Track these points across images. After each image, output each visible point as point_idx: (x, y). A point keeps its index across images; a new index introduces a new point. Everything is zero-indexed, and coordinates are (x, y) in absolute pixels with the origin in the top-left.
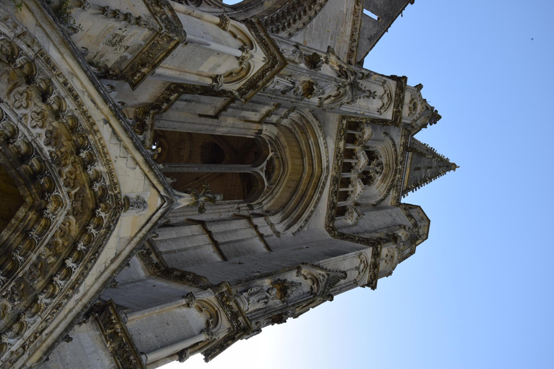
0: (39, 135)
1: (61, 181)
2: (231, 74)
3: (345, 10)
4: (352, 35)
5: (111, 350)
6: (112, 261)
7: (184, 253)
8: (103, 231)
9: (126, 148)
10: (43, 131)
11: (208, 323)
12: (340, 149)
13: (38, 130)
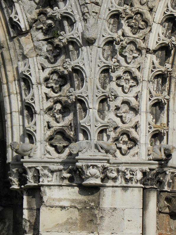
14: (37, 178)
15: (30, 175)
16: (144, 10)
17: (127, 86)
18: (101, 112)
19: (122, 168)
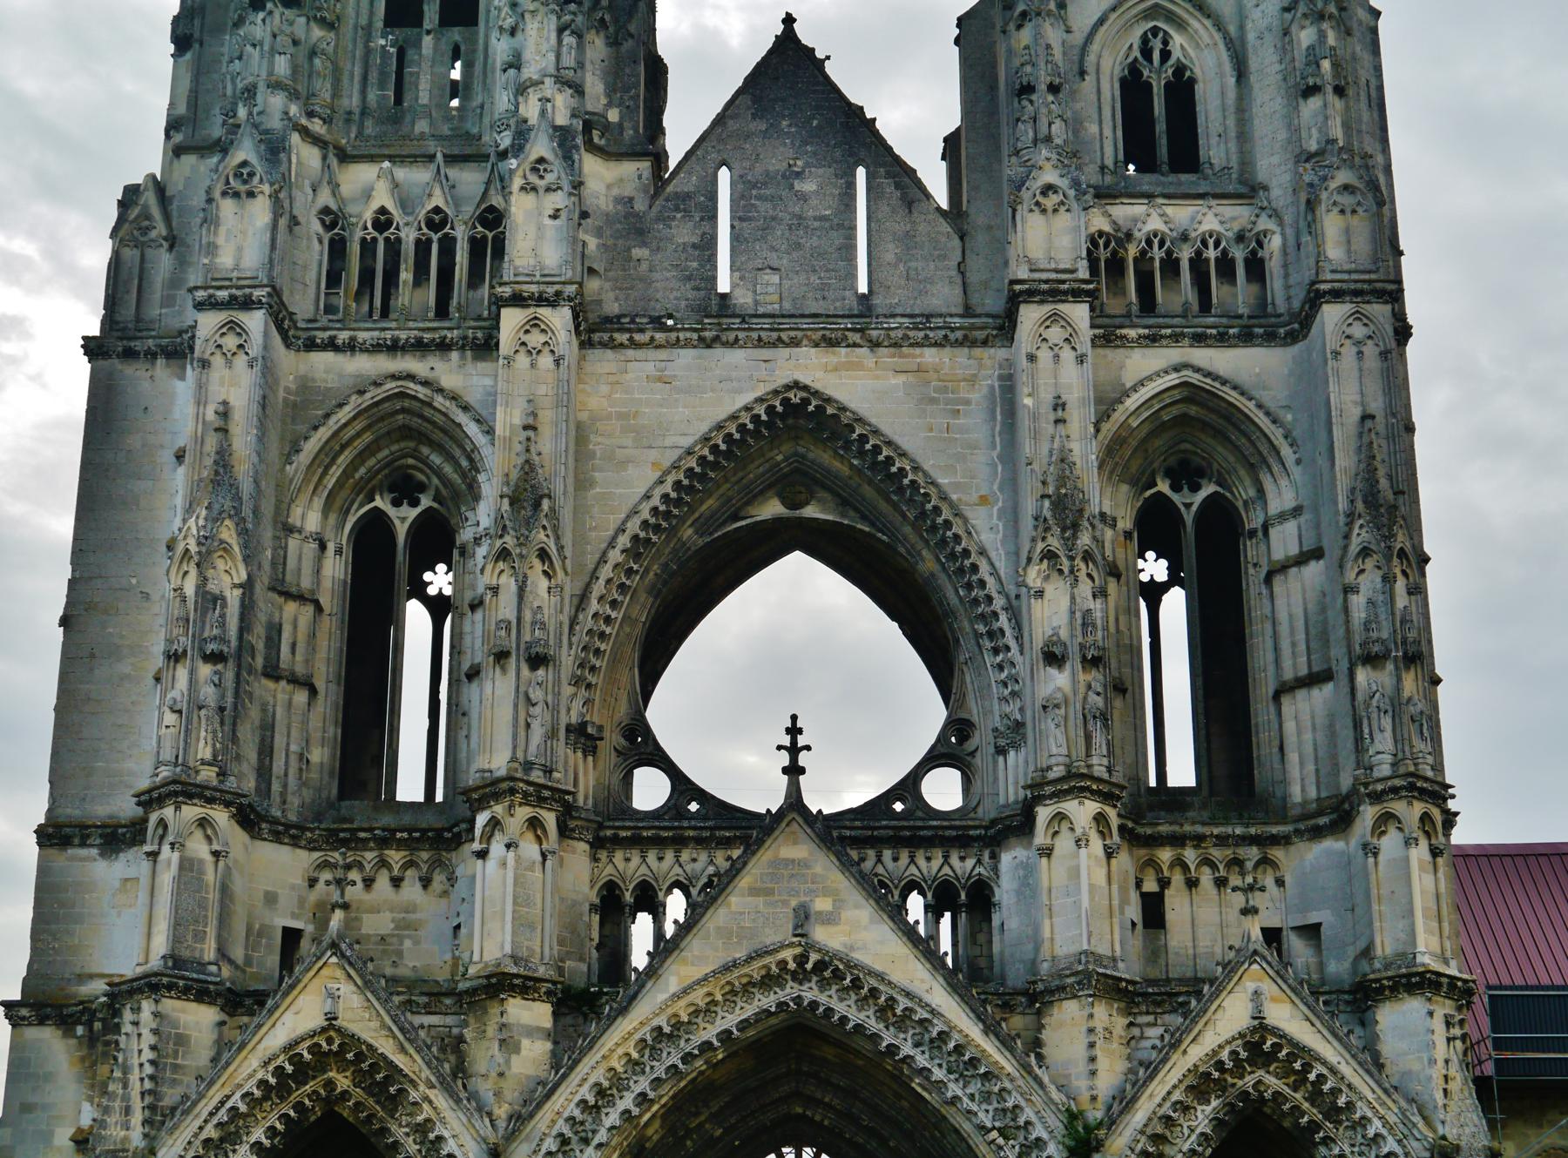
1: (1240, 1083)
2: (1101, 833)
3: (902, 378)
4: (936, 345)
5: (1406, 995)
6: (1313, 1025)
7: (1320, 754)
10: (1199, 1108)
11: (1399, 829)
12: (1140, 337)
13: (1199, 1113)
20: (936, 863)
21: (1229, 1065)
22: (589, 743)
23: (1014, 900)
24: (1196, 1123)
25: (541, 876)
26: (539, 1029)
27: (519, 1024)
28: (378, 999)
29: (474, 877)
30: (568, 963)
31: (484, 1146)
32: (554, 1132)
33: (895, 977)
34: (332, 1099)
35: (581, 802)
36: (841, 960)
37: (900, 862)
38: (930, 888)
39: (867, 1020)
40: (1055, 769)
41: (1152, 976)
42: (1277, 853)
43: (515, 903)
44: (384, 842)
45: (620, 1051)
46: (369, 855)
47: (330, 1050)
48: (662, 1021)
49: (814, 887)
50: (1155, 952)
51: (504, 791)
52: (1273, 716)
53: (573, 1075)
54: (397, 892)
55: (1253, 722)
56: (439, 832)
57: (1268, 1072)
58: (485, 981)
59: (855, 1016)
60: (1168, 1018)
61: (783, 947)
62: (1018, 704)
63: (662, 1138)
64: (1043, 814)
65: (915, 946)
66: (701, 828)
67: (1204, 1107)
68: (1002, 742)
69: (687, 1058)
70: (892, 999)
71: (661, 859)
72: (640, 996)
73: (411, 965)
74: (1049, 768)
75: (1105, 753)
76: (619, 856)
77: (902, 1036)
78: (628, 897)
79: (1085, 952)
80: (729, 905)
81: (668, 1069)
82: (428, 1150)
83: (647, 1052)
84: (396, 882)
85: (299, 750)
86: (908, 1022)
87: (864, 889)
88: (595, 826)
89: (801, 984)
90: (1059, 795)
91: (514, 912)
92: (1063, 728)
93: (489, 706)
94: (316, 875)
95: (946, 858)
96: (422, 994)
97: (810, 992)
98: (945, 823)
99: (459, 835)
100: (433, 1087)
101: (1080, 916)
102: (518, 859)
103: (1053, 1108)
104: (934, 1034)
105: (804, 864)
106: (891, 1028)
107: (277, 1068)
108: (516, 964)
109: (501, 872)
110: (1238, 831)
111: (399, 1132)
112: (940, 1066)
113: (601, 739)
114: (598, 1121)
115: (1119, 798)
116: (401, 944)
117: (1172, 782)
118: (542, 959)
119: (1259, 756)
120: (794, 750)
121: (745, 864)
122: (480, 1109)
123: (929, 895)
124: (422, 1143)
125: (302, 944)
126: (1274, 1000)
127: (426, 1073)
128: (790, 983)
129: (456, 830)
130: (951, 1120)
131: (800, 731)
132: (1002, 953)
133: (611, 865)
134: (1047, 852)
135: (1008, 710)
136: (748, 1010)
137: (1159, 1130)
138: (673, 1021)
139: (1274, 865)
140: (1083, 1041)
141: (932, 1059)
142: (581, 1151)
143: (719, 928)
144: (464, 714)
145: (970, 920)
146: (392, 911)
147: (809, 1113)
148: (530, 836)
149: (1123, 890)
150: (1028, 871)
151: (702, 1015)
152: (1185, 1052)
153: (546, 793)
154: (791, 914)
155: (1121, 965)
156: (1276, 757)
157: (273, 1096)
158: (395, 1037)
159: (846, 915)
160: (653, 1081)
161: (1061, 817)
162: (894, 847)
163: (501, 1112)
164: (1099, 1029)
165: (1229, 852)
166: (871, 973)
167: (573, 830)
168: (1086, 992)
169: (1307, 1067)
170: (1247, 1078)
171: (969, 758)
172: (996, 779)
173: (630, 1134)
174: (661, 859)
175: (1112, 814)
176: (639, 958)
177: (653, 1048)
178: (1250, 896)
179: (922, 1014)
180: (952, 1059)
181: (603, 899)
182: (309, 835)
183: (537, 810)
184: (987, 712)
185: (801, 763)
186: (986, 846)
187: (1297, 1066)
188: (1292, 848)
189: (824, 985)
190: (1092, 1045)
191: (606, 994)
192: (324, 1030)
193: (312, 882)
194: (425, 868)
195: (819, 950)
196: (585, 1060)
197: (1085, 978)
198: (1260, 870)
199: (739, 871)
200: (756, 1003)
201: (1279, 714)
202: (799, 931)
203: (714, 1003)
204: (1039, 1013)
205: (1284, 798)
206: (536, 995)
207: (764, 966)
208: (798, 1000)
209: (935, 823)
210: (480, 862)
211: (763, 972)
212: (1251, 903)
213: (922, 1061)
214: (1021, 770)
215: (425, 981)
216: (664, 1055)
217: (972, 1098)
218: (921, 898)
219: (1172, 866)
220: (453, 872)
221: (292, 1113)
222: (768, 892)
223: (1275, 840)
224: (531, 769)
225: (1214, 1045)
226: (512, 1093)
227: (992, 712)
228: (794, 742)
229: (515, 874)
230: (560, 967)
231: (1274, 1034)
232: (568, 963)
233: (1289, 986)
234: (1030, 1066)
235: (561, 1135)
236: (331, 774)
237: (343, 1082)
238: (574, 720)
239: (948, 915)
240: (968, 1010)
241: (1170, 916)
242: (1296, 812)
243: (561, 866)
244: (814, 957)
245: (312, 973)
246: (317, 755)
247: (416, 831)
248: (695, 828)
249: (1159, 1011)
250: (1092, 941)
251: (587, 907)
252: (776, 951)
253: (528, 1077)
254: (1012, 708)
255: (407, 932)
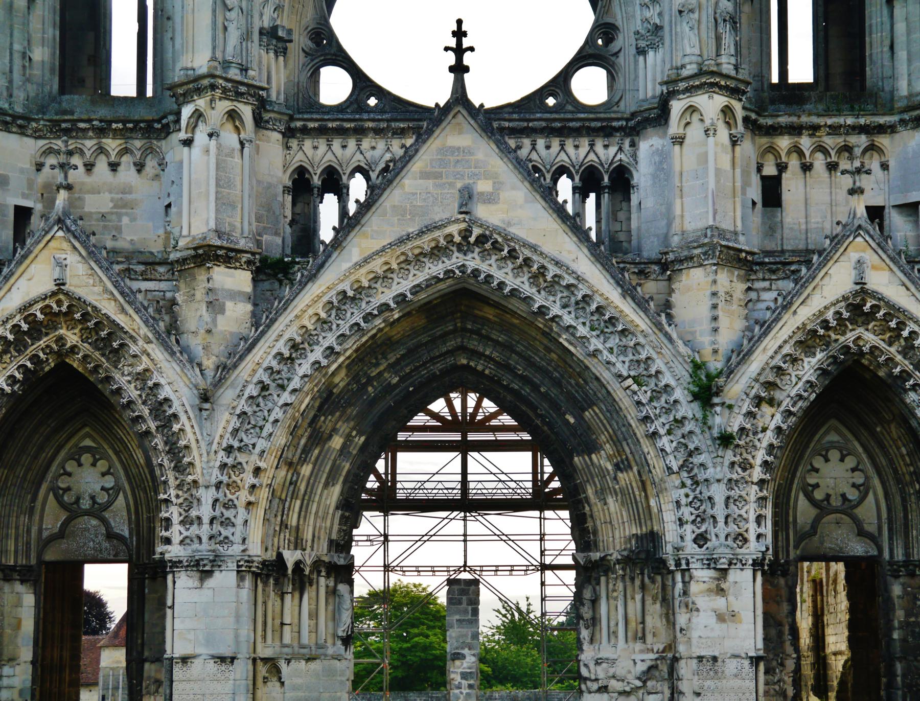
0: (809, 362)
1: (842, 339)
2: (728, 123)
6: (908, 289)
8: (882, 303)
9: (814, 288)
10: (806, 360)
13: (805, 364)
14: (688, 564)
15: (683, 562)
16: (749, 457)
17: (740, 505)
18: (726, 523)
19: (740, 557)
20: (583, 150)
21: (833, 323)
22: (280, 45)
23: (650, 183)
24: (803, 373)
25: (240, 161)
26: (241, 293)
27: (223, 289)
28: (101, 268)
29: (181, 162)
30: (265, 236)
31: (196, 392)
32: (255, 380)
33: (546, 249)
34: (63, 352)
35: (274, 97)
36: (499, 234)
37: (552, 150)
38: (577, 172)
39: (522, 285)
40: (688, 67)
41: (768, 249)
42: (883, 141)
43: (218, 185)
44: (101, 132)
45: (311, 311)
46: (89, 143)
47: (60, 311)
48: (346, 286)
49: (477, 171)
50: (771, 229)
51: (206, 87)
52: (886, 18)
53: (270, 332)
54: (114, 176)
55: (867, 25)
56: (150, 123)
57: (867, 330)
58: (192, 252)
59: (512, 282)
60: (780, 284)
61: (449, 222)
62: (658, 9)
63: (348, 384)
64: (677, 106)
65: (564, 222)
66: (379, 120)
67: (810, 359)
68: (642, 44)
69: (368, 317)
70: (543, 267)
71: (344, 147)
72: (327, 265)
73: (129, 238)
74: (683, 66)
75: (733, 52)
76: (308, 144)
77: (552, 298)
78: (316, 181)
79: (711, 227)
80: (403, 187)
81: (352, 326)
82: (148, 395)
83: (334, 312)
84: (114, 167)
85: (22, 50)
86: (557, 287)
87: (520, 173)
88: (286, 118)
89: (465, 254)
90: (690, 90)
91: (217, 192)
92: (696, 32)
93: (190, 11)
94: (42, 160)
95: (592, 145)
96: (139, 263)
97: (473, 261)
98: (592, 116)
99: (168, 124)
100: (150, 342)
101: (706, 197)
102: (219, 147)
103: (680, 359)
104: (580, 297)
105: (468, 151)
106: (543, 292)
107: (14, 326)
108: (219, 238)
109: (206, 158)
110: (850, 121)
111: (121, 379)
112: (584, 324)
113: (291, 41)
114: (291, 370)
115: (744, 93)
116: (120, 221)
117: (793, 78)
118: (242, 233)
119: (871, 55)
120: (459, 51)
121: (417, 151)
122: (191, 361)
123: (577, 178)
124: (142, 389)
125: (32, 221)
126: (874, 268)
127: (144, 330)
128: (456, 254)
129: (164, 121)
130: (593, 370)
131: (465, 34)
132: (639, 228)
133: (301, 152)
134: (679, 140)
135: (648, 14)
136: (420, 276)
137: (771, 378)
138: (356, 286)
139: (880, 151)
140: (708, 302)
141: (577, 318)
142: (278, 396)
143: (394, 206)
144: (168, 18)
145: (612, 200)
146: (110, 192)
147: (472, 364)
148: (229, 126)
149: (745, 174)
150: (662, 160)
151: (381, 280)
152: (795, 312)
153: (243, 89)
154: (457, 195)
155: (742, 238)
156: (887, 55)
157: (12, 350)
158: (116, 300)
159: (505, 195)
160: (338, 337)
161: (692, 109)
162: (547, 137)
163: (209, 363)
164: (721, 293)
165: (840, 141)
166: (525, 245)
167: (267, 122)
168: (711, 262)
169: (901, 325)
170: (849, 335)
171: (613, 59)
172: (637, 77)
173: (320, 381)
174: (344, 147)
175: (737, 106)
176: (326, 234)
177: (339, 309)
178: (857, 178)
179: (569, 280)
180: (595, 318)
181: (295, 182)
182: (34, 125)
183: (235, 103)
184: (629, 17)
185: (466, 62)
186: (627, 135)
187: (893, 324)
188: (897, 136)
189: (484, 255)
190: (715, 307)
191: (298, 263)
192: (54, 294)
193: (39, 167)
194: (138, 154)
195: (481, 226)
196: (281, 319)
197: (710, 250)
198: (868, 155)
199: (411, 157)
200: (427, 270)
201: (892, 16)
202: (464, 209)
203: (391, 270)
204: (670, 279)
205: (892, 92)
206: (238, 264)
207: (433, 240)
208: (463, 268)
209: (582, 116)
210: (186, 149)
211: (433, 244)
212: (858, 184)
213: (568, 319)
214: (659, 69)
215: (141, 252)
216: (349, 315)
217: (611, 350)
218: (569, 181)
219: (789, 153)
220: (164, 159)
221: (29, 364)
222: (438, 176)
223: (881, 129)
224: (229, 67)
225: (821, 307)
226: (219, 348)
227: (634, 16)
228: (459, 43)
229: (217, 159)
230: (258, 241)
231: (874, 298)
232: (265, 236)
233: (889, 256)
234: (660, 324)
235: (261, 382)
236: (52, 70)
237: (72, 337)
238: (266, 25)
239: (593, 196)
240: (608, 277)
241: (786, 197)
242: (899, 105)
243: (258, 154)
244: (476, 232)
245: (41, 245)
246: (40, 54)
247: (130, 122)
248: (373, 120)
249: (774, 277)
250: (717, 218)
251: (281, 189)
252: (444, 226)
253: (231, 333)
254: (652, 14)
255: (124, 211)
